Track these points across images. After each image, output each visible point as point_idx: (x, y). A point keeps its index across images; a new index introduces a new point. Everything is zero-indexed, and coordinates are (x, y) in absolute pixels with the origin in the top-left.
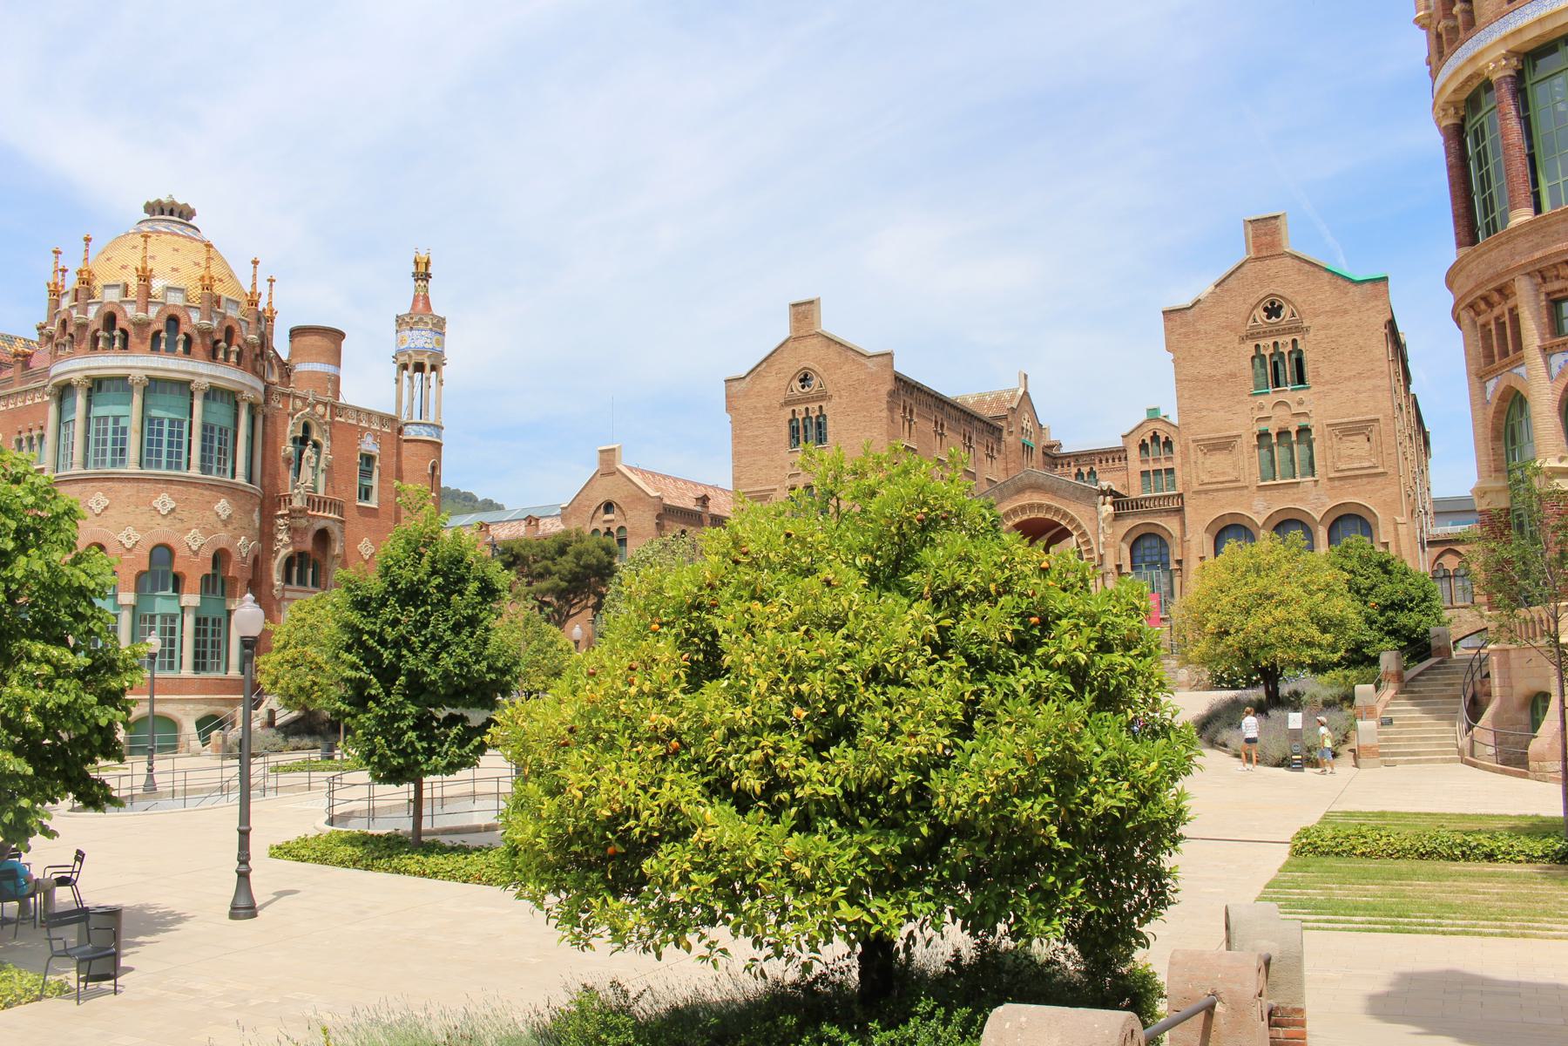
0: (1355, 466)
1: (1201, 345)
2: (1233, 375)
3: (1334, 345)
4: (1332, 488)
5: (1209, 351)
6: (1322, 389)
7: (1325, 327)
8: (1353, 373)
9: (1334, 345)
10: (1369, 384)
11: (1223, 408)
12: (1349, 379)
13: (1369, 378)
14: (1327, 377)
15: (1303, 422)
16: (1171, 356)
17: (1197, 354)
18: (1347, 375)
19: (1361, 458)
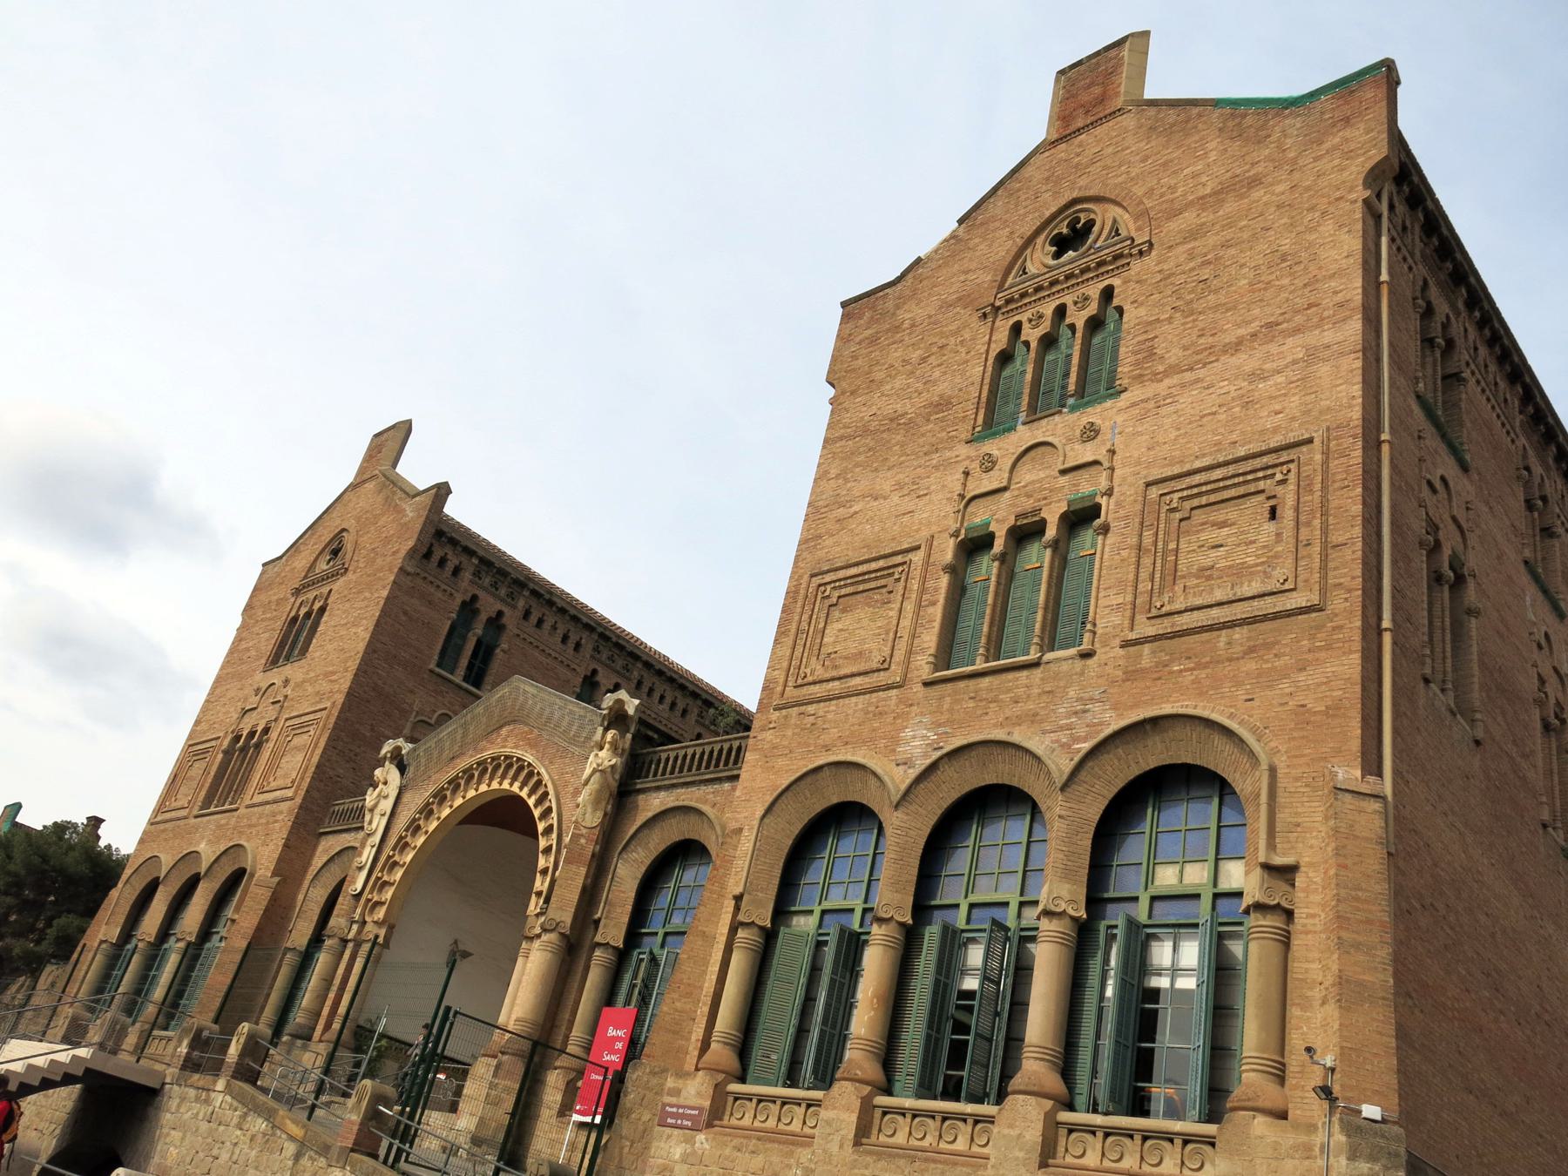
0: (1219, 595)
1: (896, 354)
2: (943, 404)
3: (1206, 273)
4: (1131, 675)
5: (905, 362)
6: (1150, 389)
7: (1193, 234)
8: (1255, 326)
9: (1206, 273)
10: (1293, 347)
11: (899, 486)
12: (1237, 346)
13: (1297, 330)
14: (1174, 355)
15: (1087, 485)
16: (831, 392)
17: (879, 375)
18: (1230, 338)
19: (1240, 572)
